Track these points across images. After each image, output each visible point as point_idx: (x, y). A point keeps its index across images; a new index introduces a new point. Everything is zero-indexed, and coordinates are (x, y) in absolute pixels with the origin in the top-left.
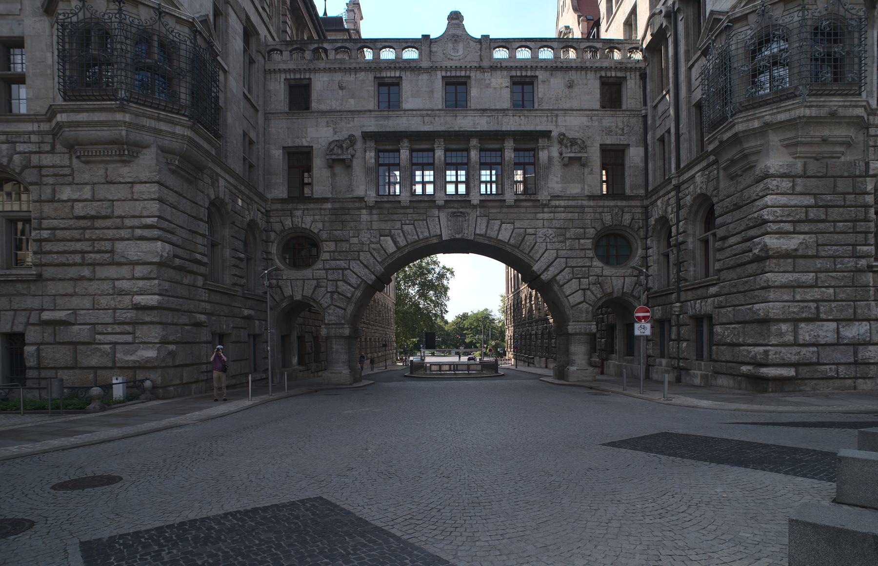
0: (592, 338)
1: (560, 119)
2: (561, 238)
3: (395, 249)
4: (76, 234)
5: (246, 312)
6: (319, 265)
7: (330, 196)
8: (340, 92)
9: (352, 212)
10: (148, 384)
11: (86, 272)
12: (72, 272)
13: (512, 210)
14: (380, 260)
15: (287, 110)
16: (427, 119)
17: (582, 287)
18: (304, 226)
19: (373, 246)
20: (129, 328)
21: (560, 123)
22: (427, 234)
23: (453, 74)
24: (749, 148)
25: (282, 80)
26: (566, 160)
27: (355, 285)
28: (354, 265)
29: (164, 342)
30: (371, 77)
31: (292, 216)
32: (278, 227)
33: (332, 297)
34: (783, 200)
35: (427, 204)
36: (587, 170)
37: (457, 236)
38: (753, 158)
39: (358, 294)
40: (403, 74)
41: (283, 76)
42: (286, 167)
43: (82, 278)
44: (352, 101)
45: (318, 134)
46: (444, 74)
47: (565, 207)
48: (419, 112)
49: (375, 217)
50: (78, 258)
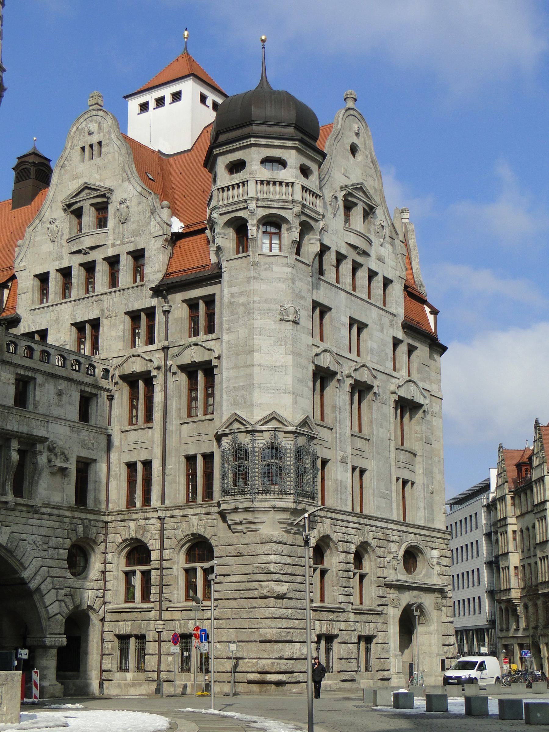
0: (61, 651)
1: (51, 426)
2: (45, 547)
13: (10, 513)
17: (60, 598)
21: (50, 430)
24: (258, 518)
26: (56, 469)
34: (278, 559)
36: (66, 480)
38: (259, 525)
47: (50, 515)
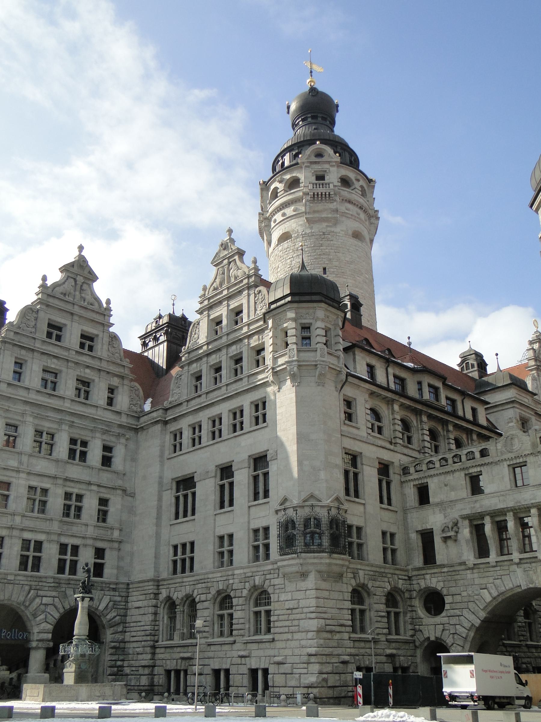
3: (490, 599)
4: (286, 617)
5: (389, 651)
6: (444, 614)
7: (446, 562)
8: (445, 488)
9: (461, 572)
10: (311, 696)
11: (289, 636)
12: (285, 636)
14: (482, 608)
15: (417, 504)
16: (501, 498)
18: (432, 586)
19: (476, 597)
20: (305, 665)
22: (511, 586)
23: (515, 462)
25: (412, 486)
27: (468, 628)
28: (465, 612)
29: (321, 673)
30: (462, 474)
31: (424, 579)
32: (416, 587)
33: (453, 638)
35: (508, 563)
37: (531, 586)
39: (472, 634)
40: (482, 469)
41: (412, 483)
42: (420, 544)
43: (288, 640)
44: (453, 493)
45: (434, 519)
46: (508, 463)
48: (495, 494)
49: (476, 575)
50: (286, 630)
